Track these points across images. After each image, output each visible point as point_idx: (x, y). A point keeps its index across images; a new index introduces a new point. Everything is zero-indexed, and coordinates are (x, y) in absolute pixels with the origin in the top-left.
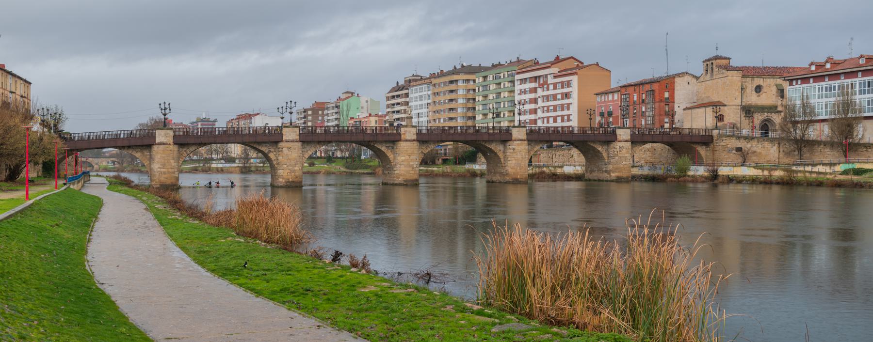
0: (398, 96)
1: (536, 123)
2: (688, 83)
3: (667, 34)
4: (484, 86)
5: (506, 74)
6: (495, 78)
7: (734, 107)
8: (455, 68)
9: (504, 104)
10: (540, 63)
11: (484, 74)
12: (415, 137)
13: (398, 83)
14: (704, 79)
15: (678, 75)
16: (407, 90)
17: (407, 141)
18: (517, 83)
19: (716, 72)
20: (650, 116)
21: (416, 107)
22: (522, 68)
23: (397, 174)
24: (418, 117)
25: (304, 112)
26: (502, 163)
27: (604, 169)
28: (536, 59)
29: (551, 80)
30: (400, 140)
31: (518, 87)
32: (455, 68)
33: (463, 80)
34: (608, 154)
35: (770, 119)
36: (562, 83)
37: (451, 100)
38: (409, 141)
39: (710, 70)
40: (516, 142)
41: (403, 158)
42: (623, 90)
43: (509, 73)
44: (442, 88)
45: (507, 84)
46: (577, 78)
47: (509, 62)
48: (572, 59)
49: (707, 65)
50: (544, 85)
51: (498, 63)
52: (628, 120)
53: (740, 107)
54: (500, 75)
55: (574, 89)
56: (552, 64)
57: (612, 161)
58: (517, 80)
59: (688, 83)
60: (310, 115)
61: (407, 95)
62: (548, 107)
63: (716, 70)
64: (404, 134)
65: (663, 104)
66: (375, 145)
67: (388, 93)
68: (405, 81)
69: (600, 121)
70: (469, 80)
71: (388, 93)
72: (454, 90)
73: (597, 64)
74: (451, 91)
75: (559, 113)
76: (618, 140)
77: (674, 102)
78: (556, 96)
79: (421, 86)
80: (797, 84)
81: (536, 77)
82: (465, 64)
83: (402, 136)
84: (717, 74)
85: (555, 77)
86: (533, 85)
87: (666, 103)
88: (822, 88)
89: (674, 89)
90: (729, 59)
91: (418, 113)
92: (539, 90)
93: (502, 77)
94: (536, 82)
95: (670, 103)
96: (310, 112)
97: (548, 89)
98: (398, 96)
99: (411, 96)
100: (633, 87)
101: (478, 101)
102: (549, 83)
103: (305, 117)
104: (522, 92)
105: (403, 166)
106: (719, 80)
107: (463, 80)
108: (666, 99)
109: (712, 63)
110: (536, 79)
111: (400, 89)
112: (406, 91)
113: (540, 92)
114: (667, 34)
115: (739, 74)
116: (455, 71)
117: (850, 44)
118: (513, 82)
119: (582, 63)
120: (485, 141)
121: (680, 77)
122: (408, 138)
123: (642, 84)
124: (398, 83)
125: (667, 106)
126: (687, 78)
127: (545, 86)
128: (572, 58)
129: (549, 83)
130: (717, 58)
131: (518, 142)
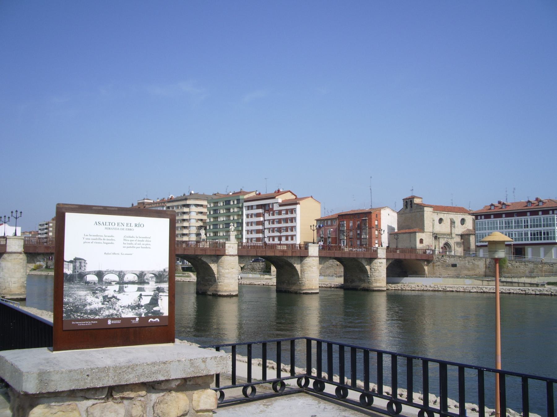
7: (429, 233)
13: (133, 205)
14: (404, 212)
17: (230, 255)
29: (276, 208)
30: (224, 255)
32: (184, 195)
35: (448, 243)
39: (409, 206)
45: (236, 210)
48: (289, 193)
49: (407, 202)
53: (432, 234)
60: (51, 227)
62: (274, 228)
66: (202, 259)
80: (481, 219)
81: (262, 205)
82: (193, 192)
84: (415, 209)
88: (502, 222)
89: (380, 219)
97: (273, 215)
102: (274, 210)
106: (418, 213)
108: (376, 225)
109: (411, 201)
113: (267, 216)
114: (371, 177)
117: (514, 192)
124: (133, 205)
127: (271, 212)
128: (290, 191)
129: (274, 210)
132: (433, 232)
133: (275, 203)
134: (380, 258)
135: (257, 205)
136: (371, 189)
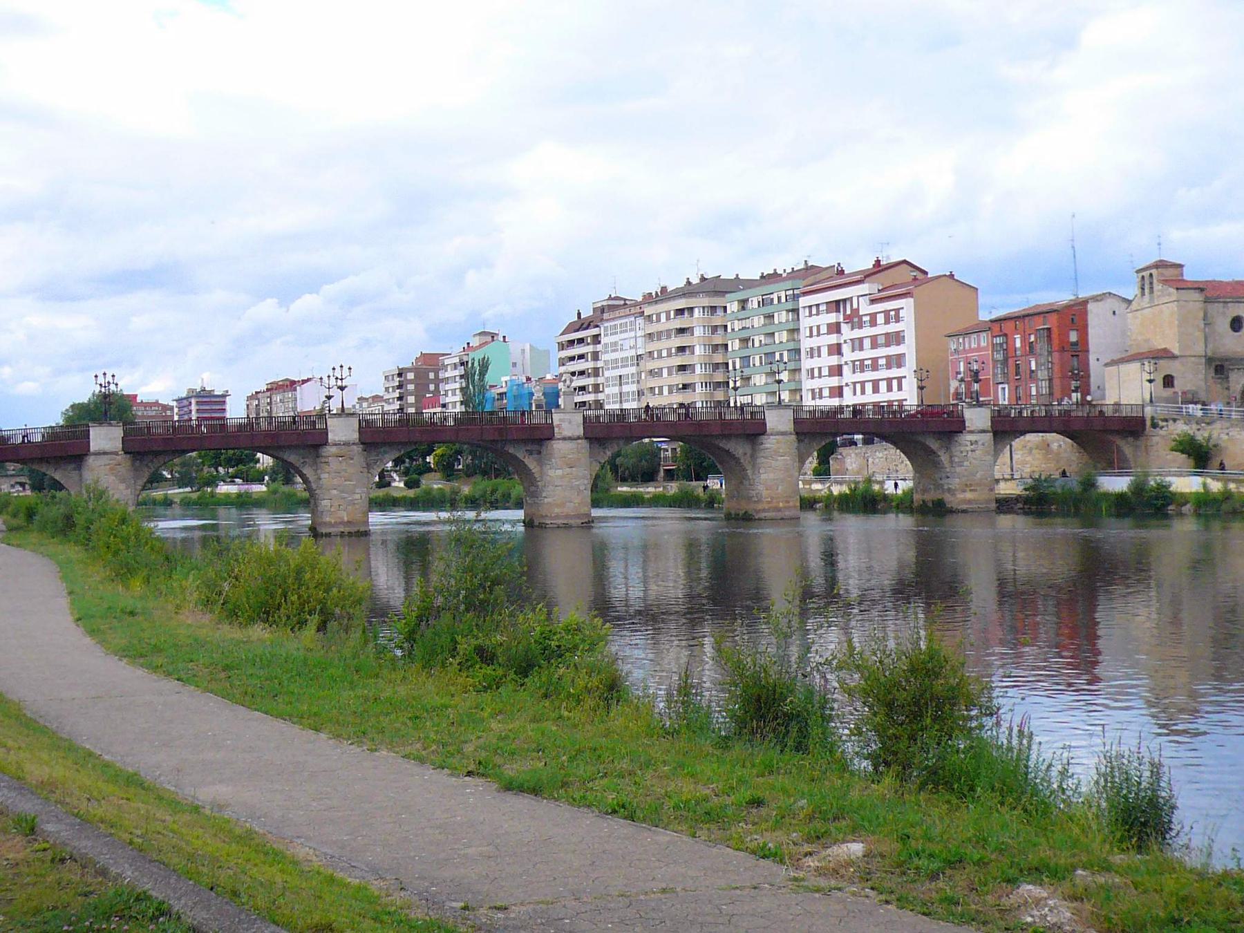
0: (581, 341)
1: (841, 395)
2: (1114, 313)
3: (1074, 216)
4: (742, 319)
5: (783, 295)
6: (763, 303)
8: (689, 283)
9: (781, 355)
10: (846, 272)
11: (741, 295)
12: (581, 431)
13: (579, 314)
14: (1139, 304)
15: (1096, 299)
16: (598, 329)
17: (564, 439)
18: (803, 313)
19: (1158, 291)
20: (1045, 380)
21: (615, 364)
22: (810, 283)
23: (548, 503)
24: (621, 385)
25: (400, 375)
26: (750, 479)
27: (946, 487)
28: (839, 264)
30: (551, 437)
31: (806, 322)
32: (689, 283)
33: (704, 308)
34: (951, 457)
36: (887, 313)
37: (681, 349)
38: (570, 439)
39: (1147, 291)
40: (774, 437)
41: (559, 472)
42: (996, 327)
43: (788, 293)
44: (664, 325)
46: (913, 304)
47: (789, 270)
48: (905, 266)
49: (1143, 277)
50: (854, 319)
51: (772, 272)
52: (1006, 386)
54: (772, 296)
55: (907, 325)
56: (866, 276)
57: (958, 469)
58: (804, 307)
59: (1114, 313)
60: (411, 382)
61: (596, 339)
63: (1158, 287)
64: (558, 426)
65: (1067, 355)
67: (562, 334)
68: (594, 309)
69: (957, 389)
70: (716, 307)
71: (562, 334)
72: (688, 328)
73: (952, 276)
74: (681, 331)
75: (883, 374)
76: (967, 429)
77: (1087, 351)
78: (876, 339)
79: (623, 321)
81: (837, 302)
83: (556, 430)
84: (1159, 296)
85: (873, 301)
86: (832, 318)
87: (1074, 353)
90: (1181, 266)
91: (620, 376)
92: (845, 328)
93: (776, 301)
94: (838, 311)
95: (1080, 353)
96: (411, 376)
97: (861, 327)
98: (581, 341)
99: (604, 340)
100: (1013, 322)
101: (733, 351)
102: (861, 313)
103: (400, 387)
104: (814, 332)
105: (560, 488)
107: (704, 308)
108: (1073, 344)
110: (836, 305)
111: (584, 326)
112: (594, 331)
113: (847, 333)
114: (1074, 216)
115: (1197, 296)
116: (689, 290)
118: (795, 311)
119: (925, 273)
120: (717, 437)
121: (1097, 300)
122: (567, 433)
123: (1028, 315)
124: (579, 314)
125: (1075, 359)
126: (1110, 304)
127: (856, 320)
128: (905, 262)
129: (861, 313)
130: (1161, 265)
131: (777, 437)
132: (1205, 356)
133: (862, 296)
134: (972, 432)
135: (827, 303)
136: (1073, 247)
